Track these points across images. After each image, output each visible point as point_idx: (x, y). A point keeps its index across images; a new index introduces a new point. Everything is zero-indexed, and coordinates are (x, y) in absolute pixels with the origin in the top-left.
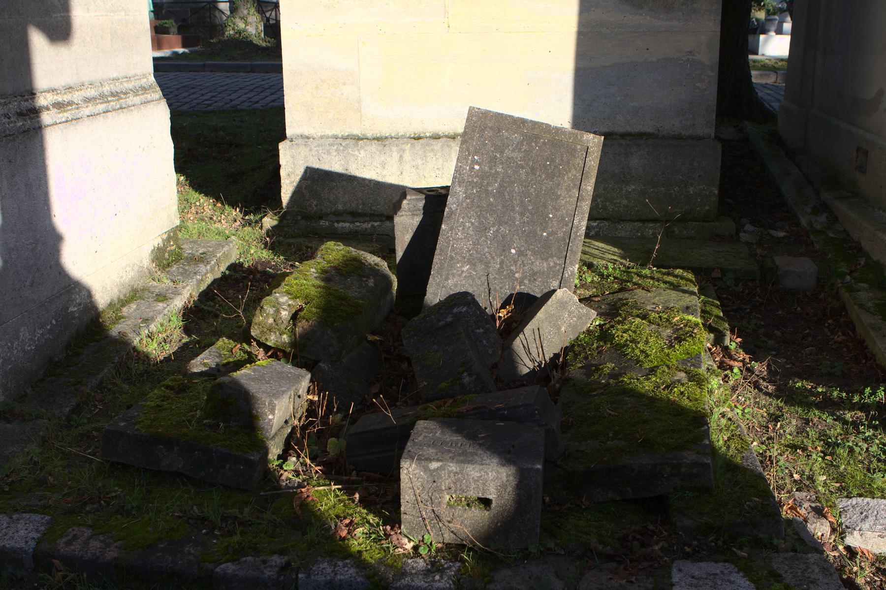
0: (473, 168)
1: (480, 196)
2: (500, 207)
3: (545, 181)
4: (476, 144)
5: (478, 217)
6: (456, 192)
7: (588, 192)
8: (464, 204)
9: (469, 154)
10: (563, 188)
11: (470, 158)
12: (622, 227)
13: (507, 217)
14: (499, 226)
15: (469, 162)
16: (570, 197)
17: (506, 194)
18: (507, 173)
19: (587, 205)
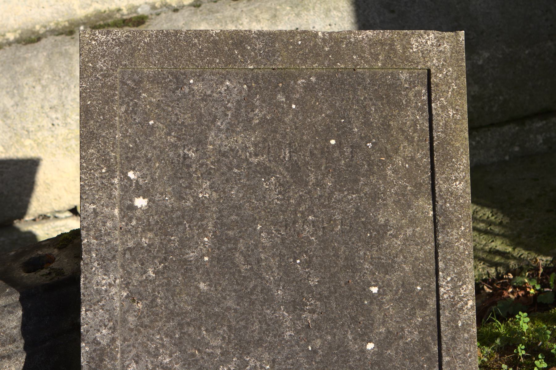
0: (132, 208)
1: (168, 284)
2: (230, 303)
3: (337, 195)
4: (125, 136)
5: (178, 344)
6: (98, 292)
7: (457, 198)
8: (131, 319)
9: (111, 172)
10: (390, 201)
11: (116, 181)
12: (478, 142)
13: (257, 326)
14: (240, 358)
15: (116, 193)
16: (413, 222)
17: (239, 258)
18: (230, 198)
19: (464, 235)
